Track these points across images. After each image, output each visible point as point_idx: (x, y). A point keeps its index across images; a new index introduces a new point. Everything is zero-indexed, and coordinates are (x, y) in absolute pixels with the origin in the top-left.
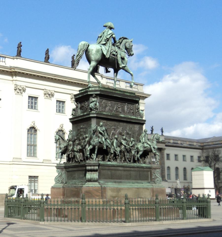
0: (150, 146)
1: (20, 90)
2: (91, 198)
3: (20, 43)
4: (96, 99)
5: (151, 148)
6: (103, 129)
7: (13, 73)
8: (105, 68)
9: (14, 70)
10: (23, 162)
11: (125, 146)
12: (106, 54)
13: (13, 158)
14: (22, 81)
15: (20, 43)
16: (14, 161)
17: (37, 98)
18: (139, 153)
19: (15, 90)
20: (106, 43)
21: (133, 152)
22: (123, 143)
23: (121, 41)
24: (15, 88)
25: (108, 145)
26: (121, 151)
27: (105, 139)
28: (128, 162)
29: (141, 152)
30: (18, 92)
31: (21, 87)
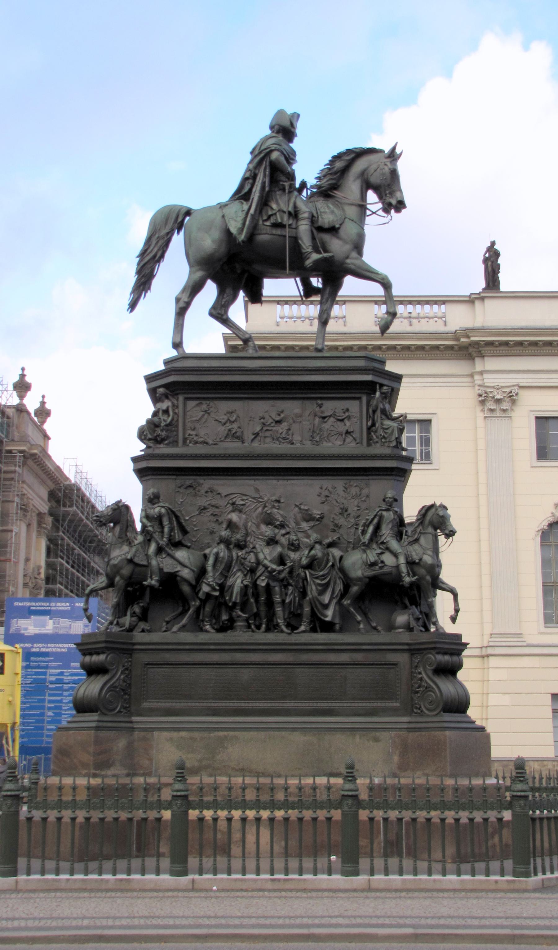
0: (396, 555)
1: (498, 401)
2: (69, 775)
3: (493, 243)
4: (170, 404)
5: (398, 567)
6: (157, 510)
7: (471, 350)
8: (298, 279)
9: (468, 337)
10: (528, 646)
11: (266, 567)
12: (242, 229)
13: (491, 634)
14: (499, 372)
15: (493, 243)
16: (491, 644)
17: (430, 421)
18: (350, 589)
19: (483, 402)
20: (250, 190)
21: (312, 590)
22: (261, 556)
23: (339, 165)
24: (480, 399)
25: (179, 568)
26: (251, 591)
27: (160, 550)
28: (282, 631)
29: (355, 585)
30: (492, 410)
31: (505, 392)
